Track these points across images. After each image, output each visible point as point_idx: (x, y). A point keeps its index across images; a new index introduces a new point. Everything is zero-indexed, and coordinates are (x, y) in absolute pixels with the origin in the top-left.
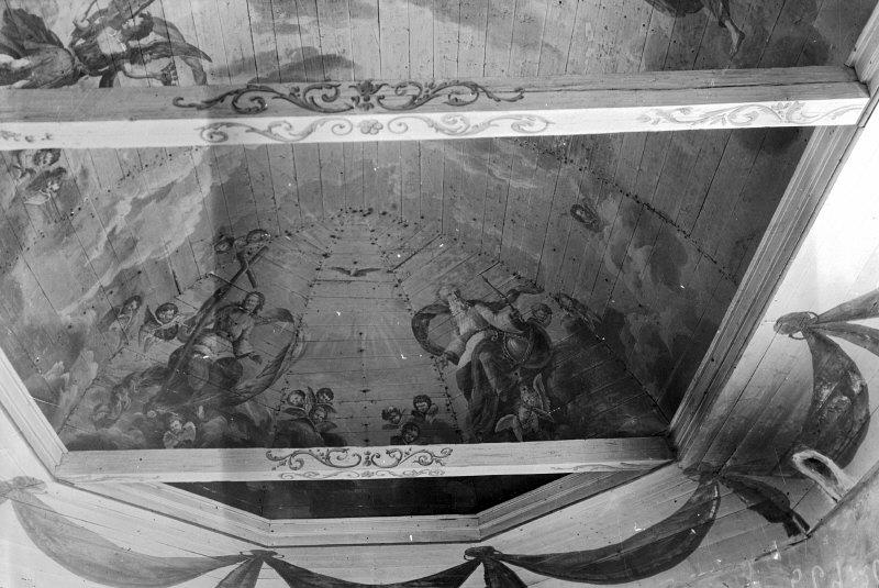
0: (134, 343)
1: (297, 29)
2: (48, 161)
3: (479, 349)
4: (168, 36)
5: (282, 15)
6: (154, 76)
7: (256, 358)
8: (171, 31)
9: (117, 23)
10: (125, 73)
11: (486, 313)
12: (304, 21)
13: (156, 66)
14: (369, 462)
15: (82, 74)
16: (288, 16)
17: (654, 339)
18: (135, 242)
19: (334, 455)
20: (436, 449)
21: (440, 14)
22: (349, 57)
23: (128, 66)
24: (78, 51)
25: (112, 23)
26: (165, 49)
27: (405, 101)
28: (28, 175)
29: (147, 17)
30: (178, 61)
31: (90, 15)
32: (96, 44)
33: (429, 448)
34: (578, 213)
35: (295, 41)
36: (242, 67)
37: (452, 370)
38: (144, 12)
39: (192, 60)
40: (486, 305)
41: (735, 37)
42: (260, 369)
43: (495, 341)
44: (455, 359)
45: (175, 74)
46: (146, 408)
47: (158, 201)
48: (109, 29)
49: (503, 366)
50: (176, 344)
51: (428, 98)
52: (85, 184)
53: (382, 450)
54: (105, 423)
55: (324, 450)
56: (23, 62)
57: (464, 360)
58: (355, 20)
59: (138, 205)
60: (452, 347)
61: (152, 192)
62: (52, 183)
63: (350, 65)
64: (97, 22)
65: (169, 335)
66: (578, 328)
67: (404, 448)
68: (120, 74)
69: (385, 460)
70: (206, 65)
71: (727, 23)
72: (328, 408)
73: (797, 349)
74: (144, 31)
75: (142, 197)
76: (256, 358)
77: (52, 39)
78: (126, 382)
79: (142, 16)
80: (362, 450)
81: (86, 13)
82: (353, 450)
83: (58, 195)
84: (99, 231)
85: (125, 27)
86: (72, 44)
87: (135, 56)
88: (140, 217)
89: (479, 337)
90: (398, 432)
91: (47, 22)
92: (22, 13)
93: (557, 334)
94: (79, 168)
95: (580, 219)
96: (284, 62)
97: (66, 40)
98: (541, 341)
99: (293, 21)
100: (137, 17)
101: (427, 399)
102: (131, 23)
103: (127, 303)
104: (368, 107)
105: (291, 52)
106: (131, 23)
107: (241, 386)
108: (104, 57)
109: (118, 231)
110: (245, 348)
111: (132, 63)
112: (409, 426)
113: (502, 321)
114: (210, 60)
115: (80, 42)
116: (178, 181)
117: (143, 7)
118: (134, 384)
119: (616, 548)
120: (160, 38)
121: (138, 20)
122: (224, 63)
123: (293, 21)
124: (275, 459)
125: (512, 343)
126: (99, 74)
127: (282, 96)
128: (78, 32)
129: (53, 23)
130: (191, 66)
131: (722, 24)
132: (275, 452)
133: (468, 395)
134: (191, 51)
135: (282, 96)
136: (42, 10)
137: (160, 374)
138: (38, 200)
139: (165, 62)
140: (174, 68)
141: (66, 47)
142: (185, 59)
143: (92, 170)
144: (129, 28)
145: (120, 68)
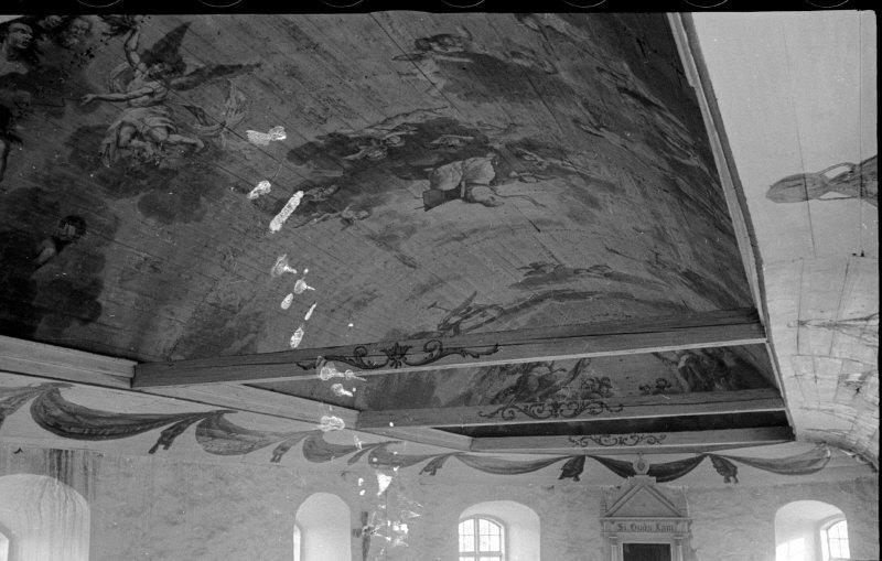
7: (564, 370)
14: (621, 443)
19: (603, 439)
20: (658, 435)
27: (571, 412)
33: (653, 434)
37: (675, 370)
42: (565, 374)
44: (677, 364)
50: (518, 375)
51: (581, 411)
55: (598, 436)
57: (681, 364)
67: (640, 435)
69: (631, 441)
72: (608, 386)
76: (564, 370)
80: (617, 436)
82: (613, 436)
104: (556, 416)
119: (782, 460)
124: (574, 441)
127: (521, 410)
132: (573, 438)
133: (686, 379)
135: (521, 410)
137: (514, 389)
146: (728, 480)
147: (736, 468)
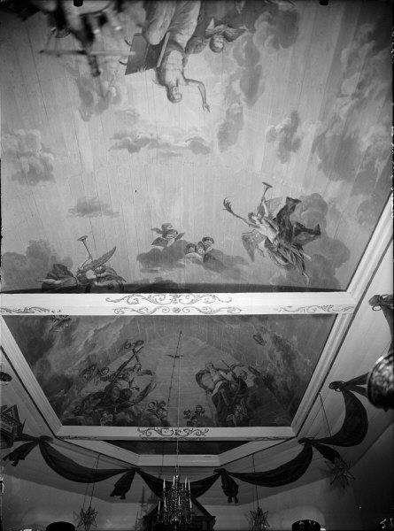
0: (92, 381)
1: (156, 271)
3: (219, 389)
7: (138, 389)
9: (93, 268)
11: (222, 373)
17: (285, 388)
24: (79, 278)
40: (223, 370)
41: (308, 279)
43: (226, 385)
44: (212, 391)
46: (95, 408)
48: (90, 271)
49: (230, 394)
50: (108, 383)
53: (182, 429)
54: (78, 414)
57: (215, 391)
59: (96, 331)
60: (211, 386)
65: (105, 380)
66: (256, 381)
73: (339, 396)
74: (103, 271)
76: (138, 389)
77: (70, 274)
78: (88, 398)
89: (221, 382)
90: (189, 420)
93: (250, 383)
97: (75, 274)
98: (244, 385)
99: (155, 269)
101: (200, 406)
103: (90, 368)
107: (131, 400)
110: (133, 385)
112: (193, 418)
113: (229, 377)
118: (91, 398)
123: (155, 269)
125: (233, 386)
137: (100, 395)
146: (230, 501)
147: (237, 486)
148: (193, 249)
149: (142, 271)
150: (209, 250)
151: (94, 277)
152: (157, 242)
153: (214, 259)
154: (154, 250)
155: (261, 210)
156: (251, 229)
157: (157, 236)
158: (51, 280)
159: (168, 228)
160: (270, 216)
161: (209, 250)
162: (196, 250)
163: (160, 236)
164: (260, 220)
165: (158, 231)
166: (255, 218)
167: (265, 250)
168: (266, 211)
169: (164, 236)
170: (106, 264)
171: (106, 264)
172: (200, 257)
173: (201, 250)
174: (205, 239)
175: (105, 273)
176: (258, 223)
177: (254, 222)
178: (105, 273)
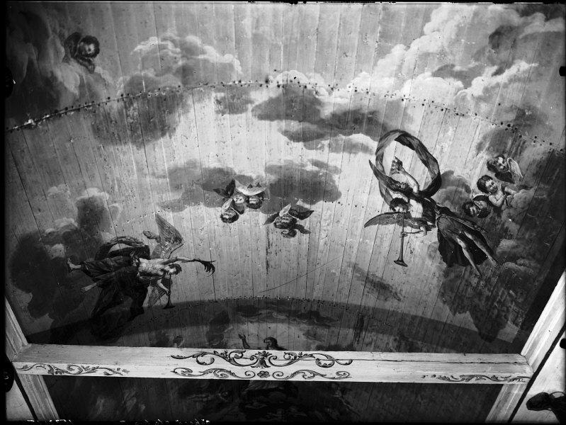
1: (316, 163)
2: (491, 181)
4: (386, 191)
5: (321, 174)
6: (405, 172)
8: (384, 192)
9: (407, 215)
10: (419, 188)
12: (310, 168)
13: (401, 178)
15: (439, 208)
16: (318, 172)
18: (492, 37)
21: (229, 171)
22: (286, 139)
23: (415, 190)
25: (410, 217)
26: (391, 184)
28: (506, 189)
29: (392, 208)
30: (388, 173)
31: (418, 230)
32: (423, 215)
34: (92, 47)
35: (313, 155)
36: (352, 148)
38: (392, 211)
39: (380, 168)
41: (72, 266)
45: (393, 165)
47: (453, 66)
52: (485, 138)
56: (462, 244)
58: (279, 164)
61: (451, 80)
62: (500, 165)
63: (286, 133)
64: (416, 224)
68: (421, 189)
70: (374, 162)
71: (79, 266)
74: (397, 202)
75: (459, 84)
79: (395, 210)
81: (418, 232)
83: (504, 152)
84: (506, 86)
85: (405, 211)
86: (434, 226)
87: (408, 192)
88: (473, 64)
91: (437, 246)
92: (445, 259)
94: (480, 155)
95: (89, 40)
96: (326, 142)
97: (435, 231)
99: (315, 169)
100: (397, 211)
102: (401, 210)
105: (320, 148)
106: (401, 210)
108: (423, 206)
109: (495, 68)
111: (412, 189)
114: (370, 161)
115: (429, 223)
116: (430, 73)
117: (392, 213)
120: (391, 192)
121: (397, 209)
122: (361, 154)
123: (315, 169)
126: (432, 200)
128: (428, 229)
129: (435, 243)
130: (381, 165)
131: (82, 263)
134: (378, 173)
136: (435, 252)
138: (516, 167)
139: (395, 177)
140: (392, 170)
141: (437, 228)
142: (383, 171)
143: (475, 144)
144: (404, 209)
145: (420, 192)
148: (253, 201)
149: (337, 170)
150: (227, 204)
151: (413, 202)
152: (305, 214)
153: (217, 191)
154: (312, 203)
155: (168, 283)
156: (174, 256)
157: (305, 223)
158: (466, 254)
159: (287, 231)
160: (154, 284)
161: (227, 204)
162: (247, 198)
163: (300, 222)
164: (165, 272)
165: (303, 230)
166: (172, 271)
167: (146, 242)
168: (161, 285)
169: (294, 221)
170: (387, 209)
171: (387, 209)
172: (240, 190)
173: (240, 201)
174: (234, 219)
175: (396, 195)
176: (167, 268)
177: (172, 267)
178: (396, 195)
